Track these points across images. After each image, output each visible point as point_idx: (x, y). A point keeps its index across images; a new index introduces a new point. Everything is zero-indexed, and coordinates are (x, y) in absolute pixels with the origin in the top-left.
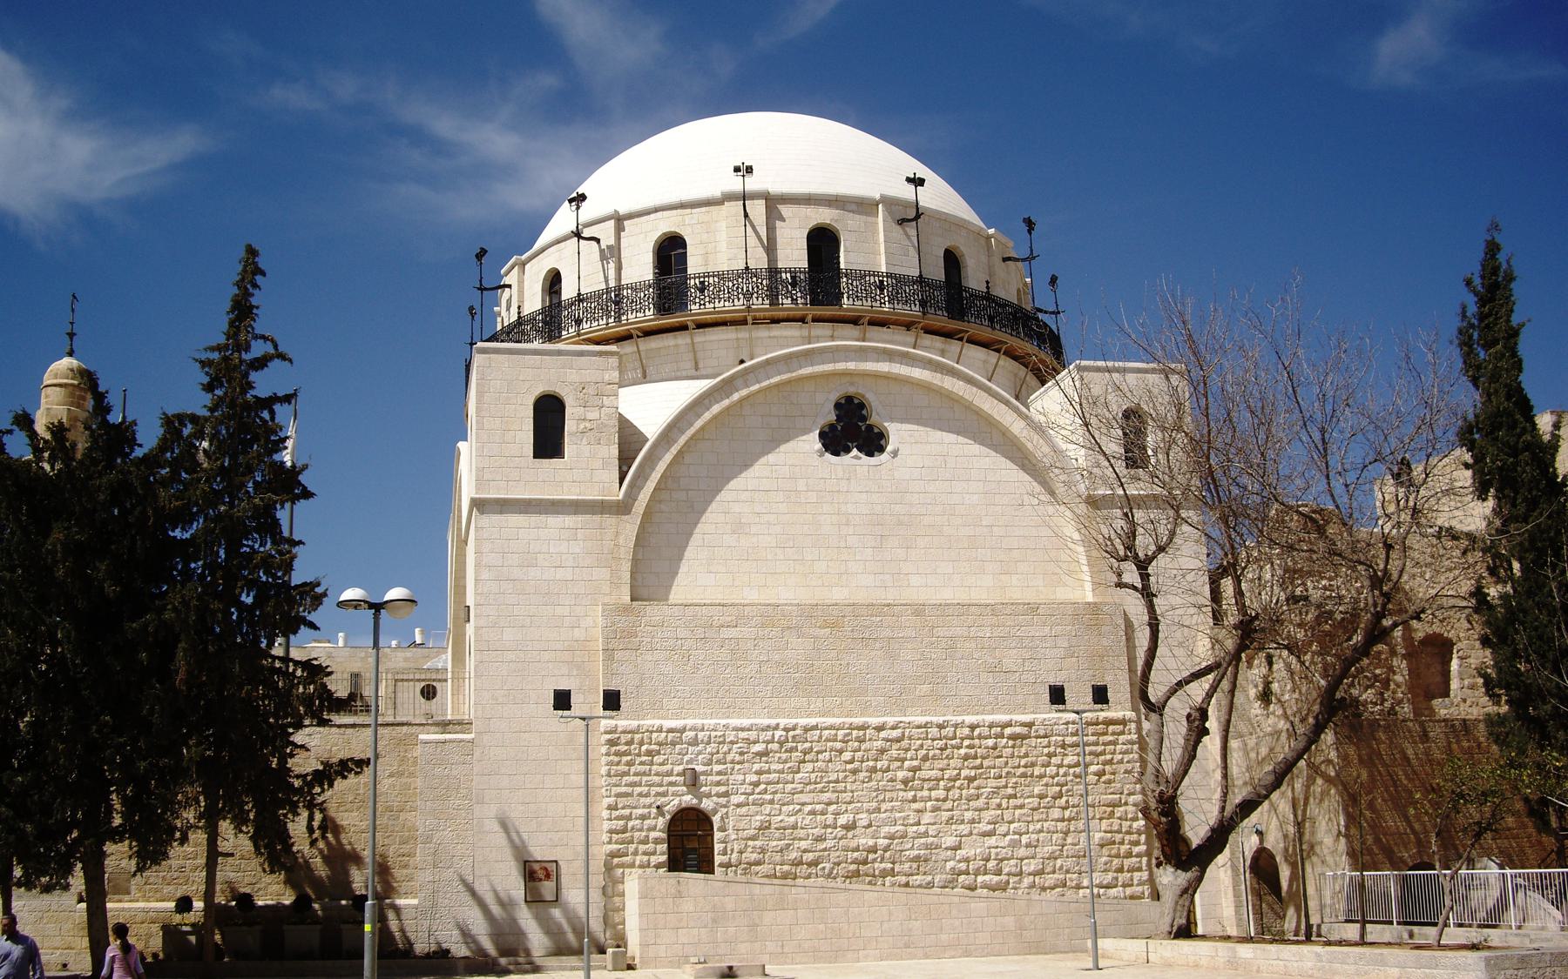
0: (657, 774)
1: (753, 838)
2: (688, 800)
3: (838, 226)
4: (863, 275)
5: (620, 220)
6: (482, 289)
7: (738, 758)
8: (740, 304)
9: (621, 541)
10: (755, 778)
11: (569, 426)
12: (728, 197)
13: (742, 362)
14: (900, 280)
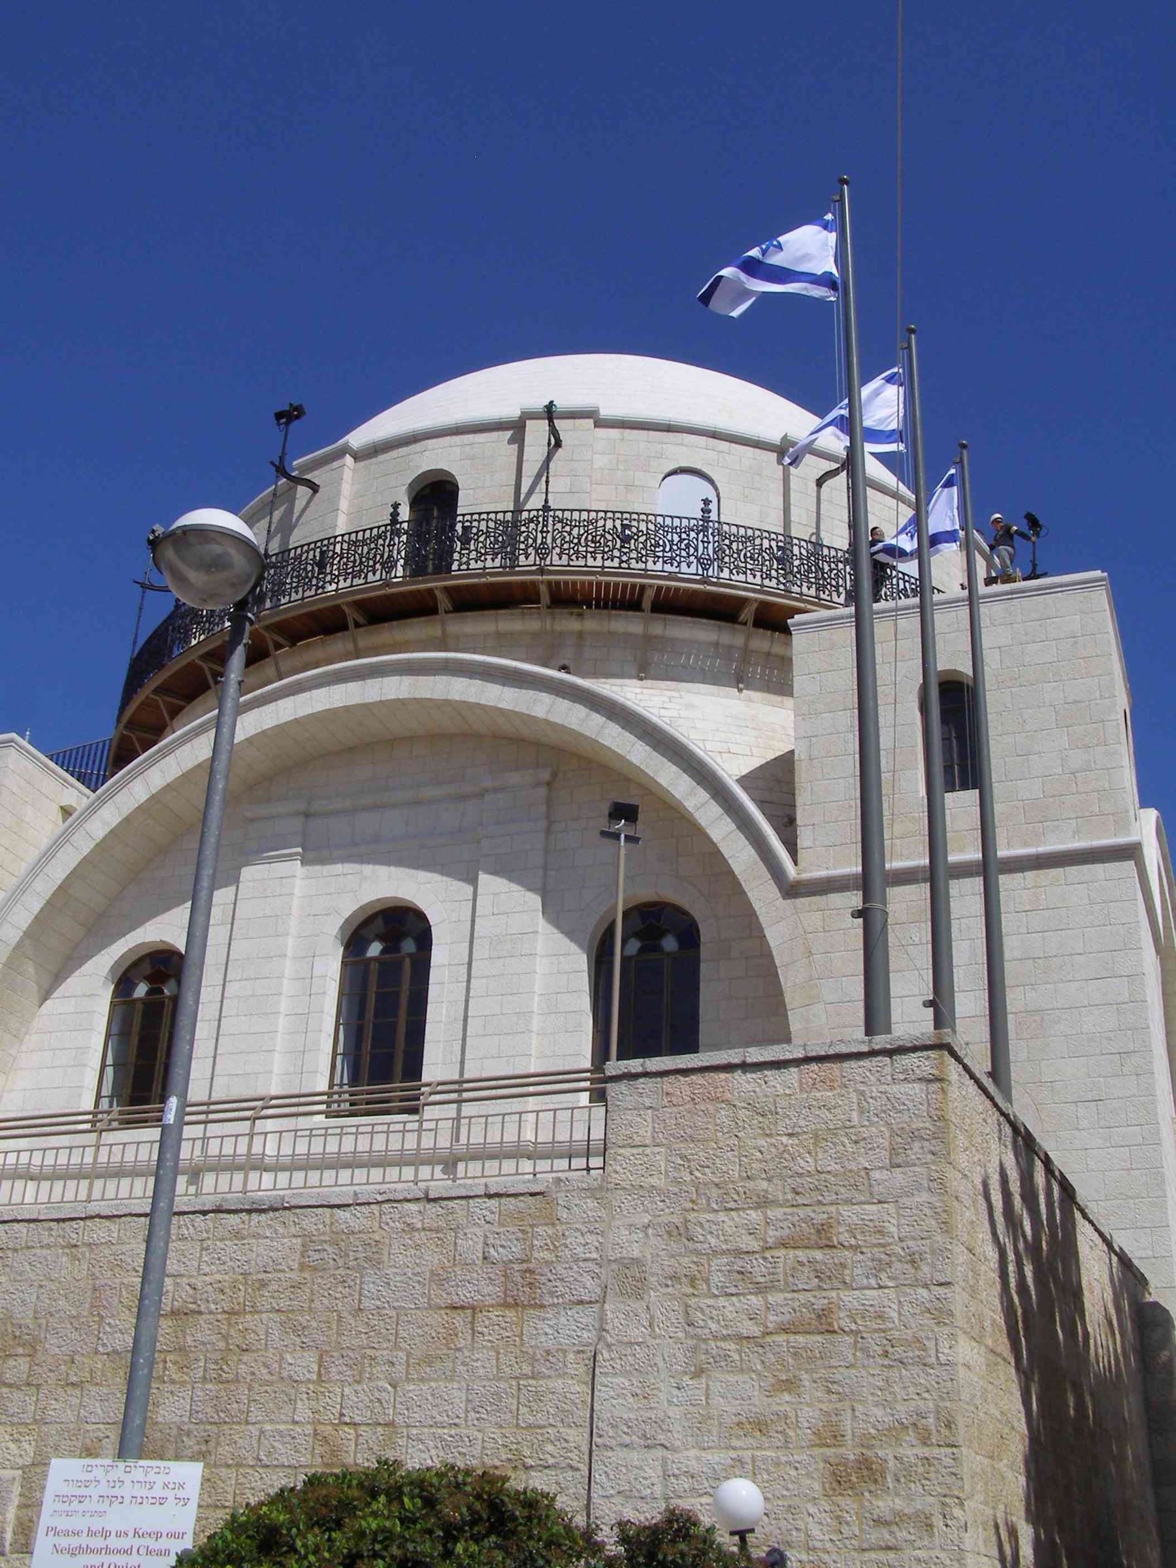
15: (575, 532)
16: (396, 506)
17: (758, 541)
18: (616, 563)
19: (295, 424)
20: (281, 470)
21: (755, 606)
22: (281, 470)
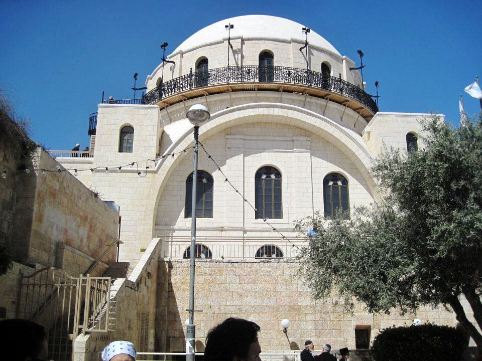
4: (280, 69)
5: (182, 54)
6: (135, 89)
8: (225, 82)
12: (225, 40)
13: (227, 108)
14: (298, 71)
15: (236, 72)
16: (191, 69)
17: (283, 70)
18: (247, 80)
19: (166, 48)
20: (164, 60)
21: (282, 87)
22: (164, 60)
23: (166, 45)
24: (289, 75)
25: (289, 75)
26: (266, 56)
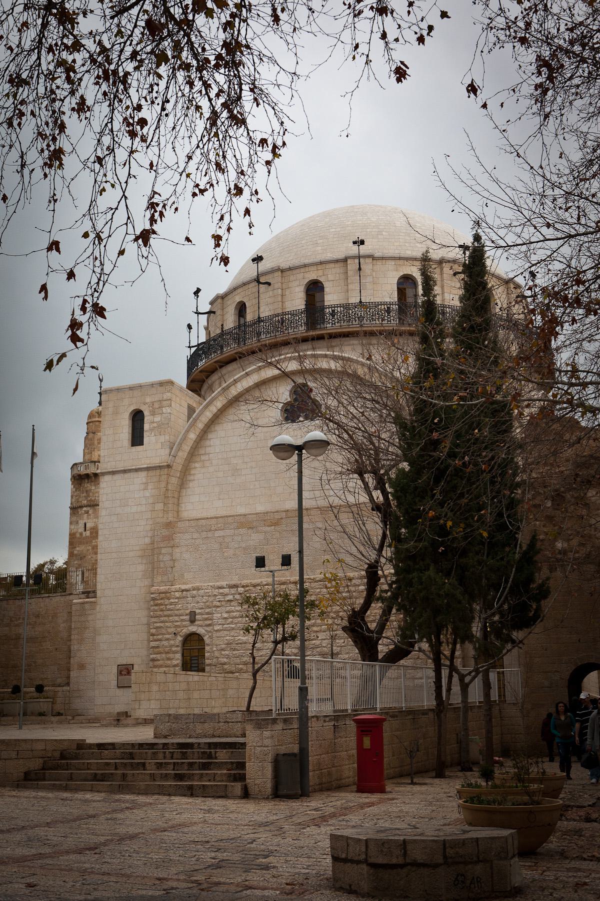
0: (176, 615)
1: (223, 650)
2: (193, 629)
3: (321, 279)
7: (218, 604)
9: (170, 488)
10: (226, 615)
11: (146, 427)
20: (198, 313)
23: (198, 290)
24: (333, 316)
25: (333, 316)
26: (314, 289)
